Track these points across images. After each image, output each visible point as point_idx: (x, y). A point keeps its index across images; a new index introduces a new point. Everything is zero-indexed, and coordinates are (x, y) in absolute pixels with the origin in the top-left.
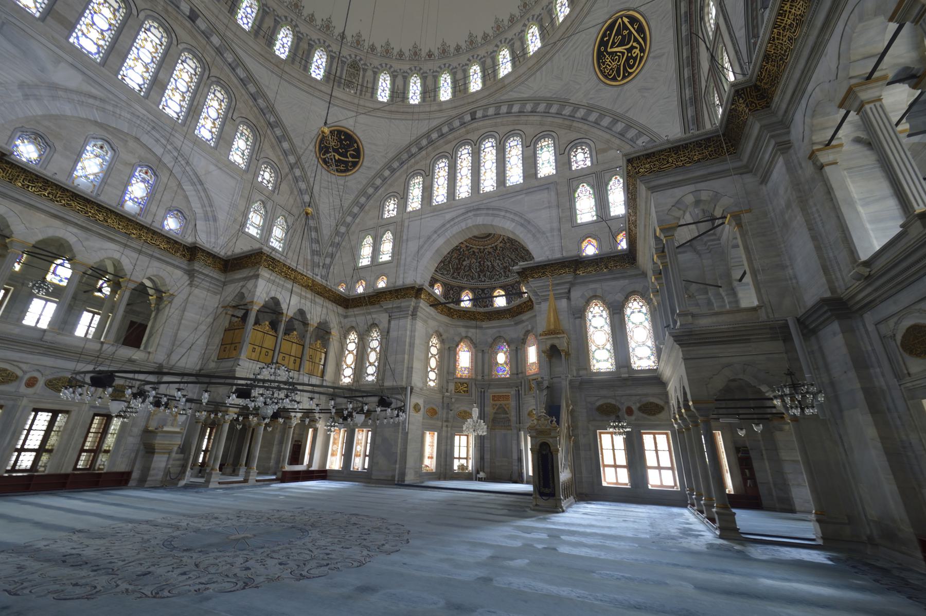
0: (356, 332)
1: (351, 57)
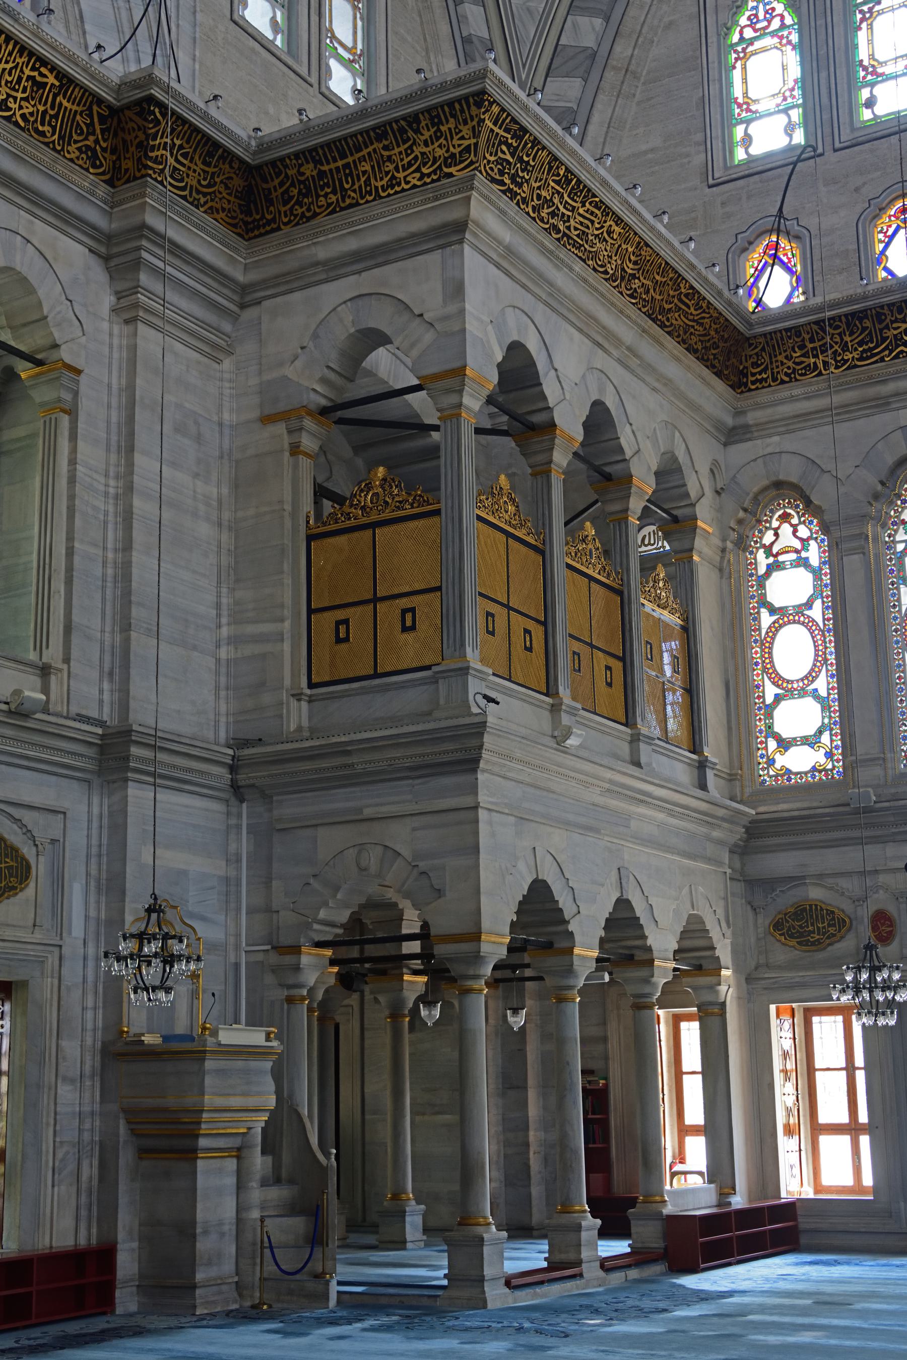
0: (810, 507)
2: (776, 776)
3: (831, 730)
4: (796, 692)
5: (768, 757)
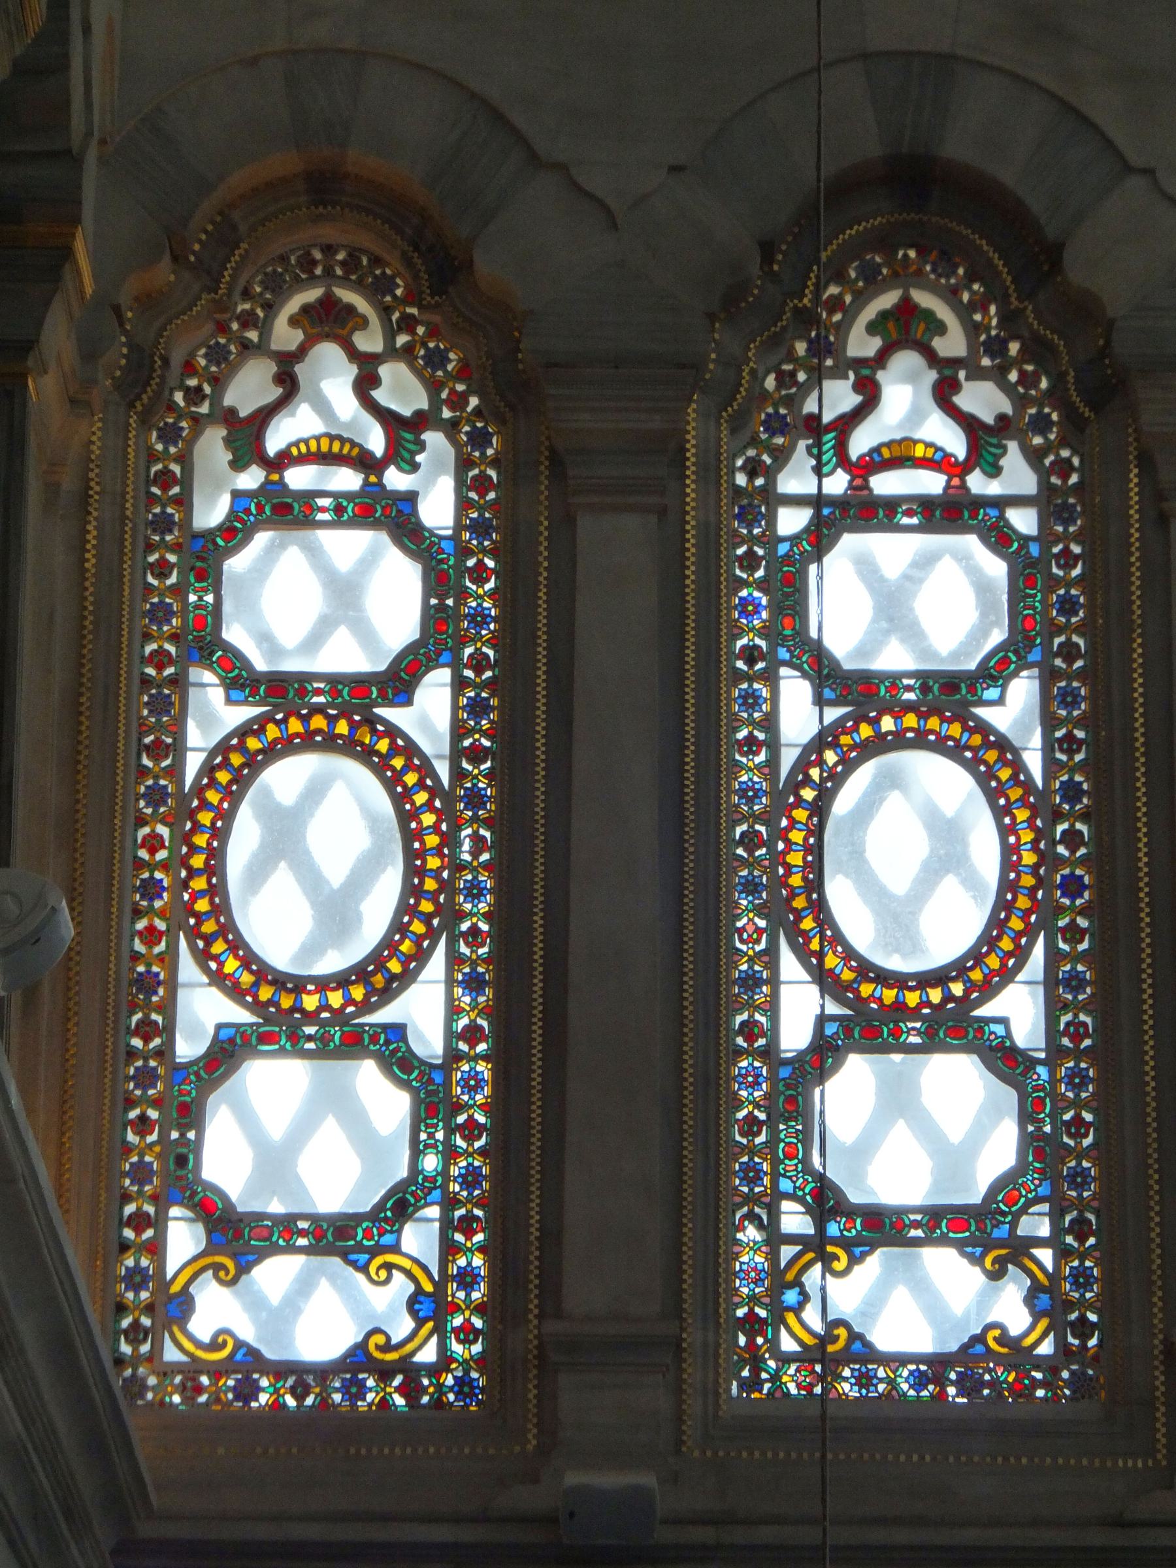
2: (193, 1368)
3: (450, 1202)
4: (310, 1030)
5: (164, 1285)
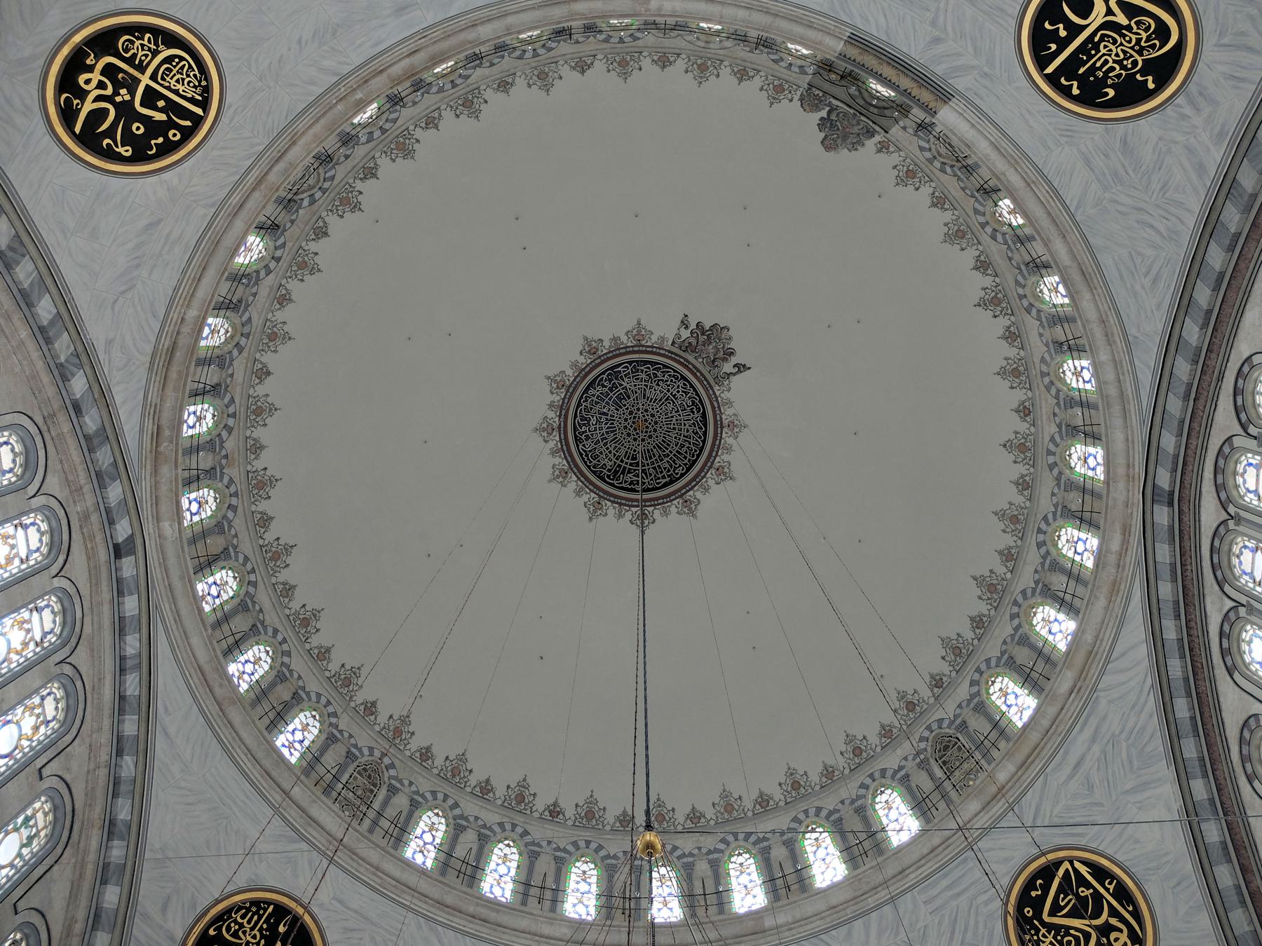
1: (371, 755)
